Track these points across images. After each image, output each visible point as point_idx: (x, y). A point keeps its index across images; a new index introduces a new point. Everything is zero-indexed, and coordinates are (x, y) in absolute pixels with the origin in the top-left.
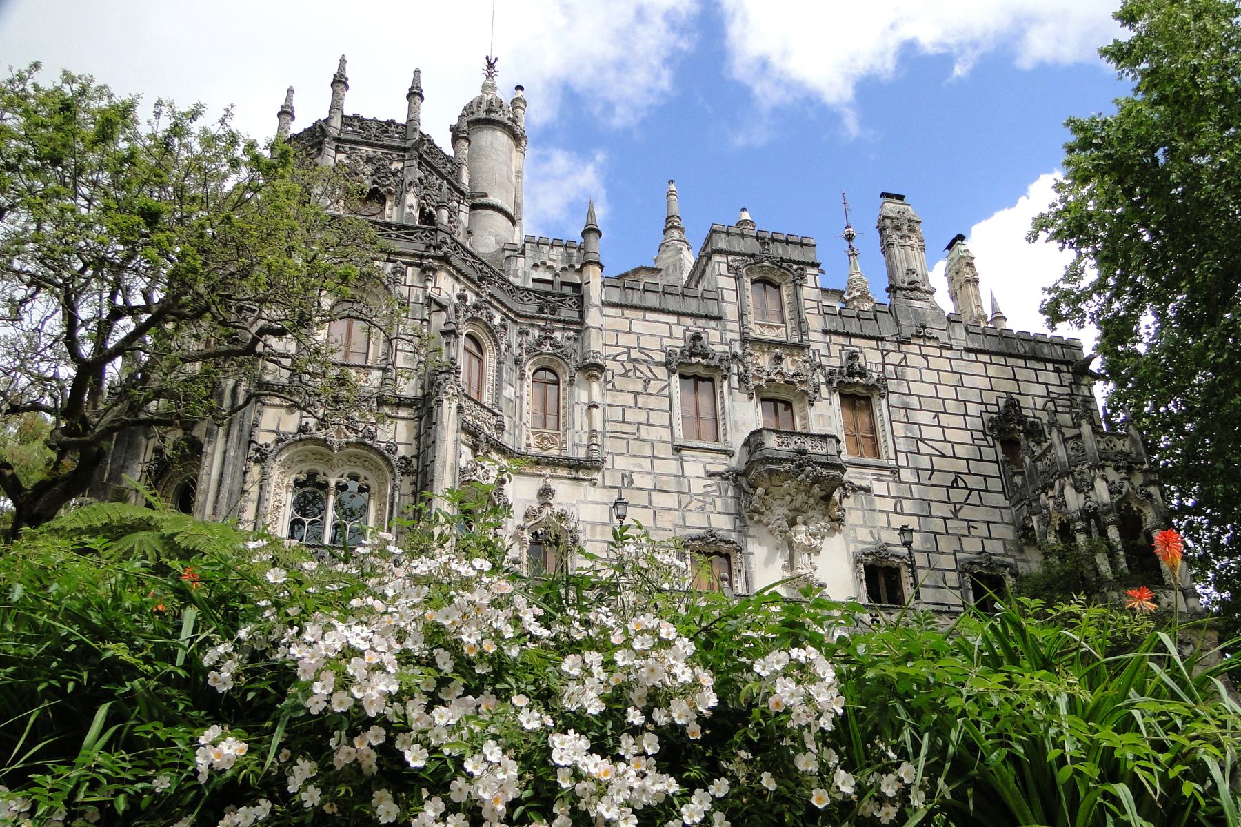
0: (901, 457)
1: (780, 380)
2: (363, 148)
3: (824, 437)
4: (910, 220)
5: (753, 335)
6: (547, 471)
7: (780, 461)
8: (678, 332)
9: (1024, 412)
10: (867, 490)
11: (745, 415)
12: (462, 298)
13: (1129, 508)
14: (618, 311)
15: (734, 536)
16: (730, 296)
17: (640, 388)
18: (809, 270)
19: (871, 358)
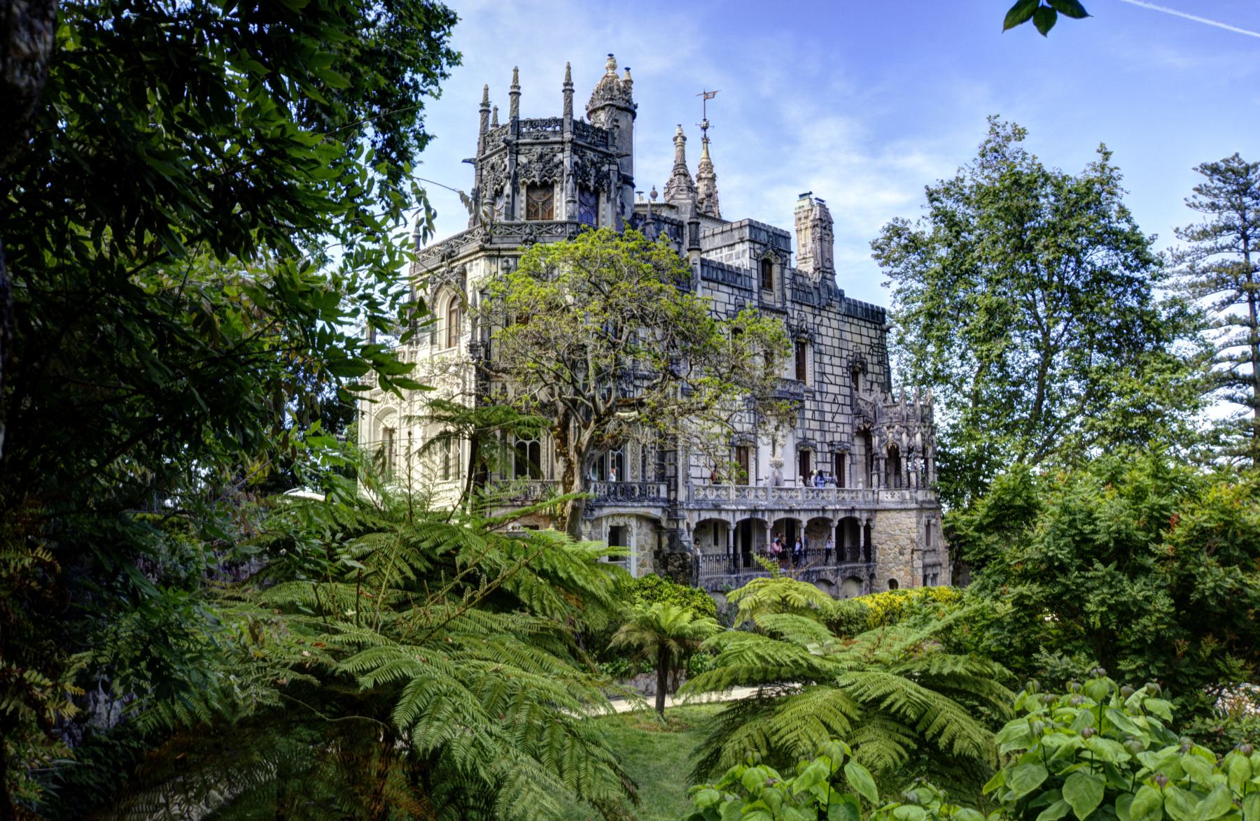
2: (588, 152)
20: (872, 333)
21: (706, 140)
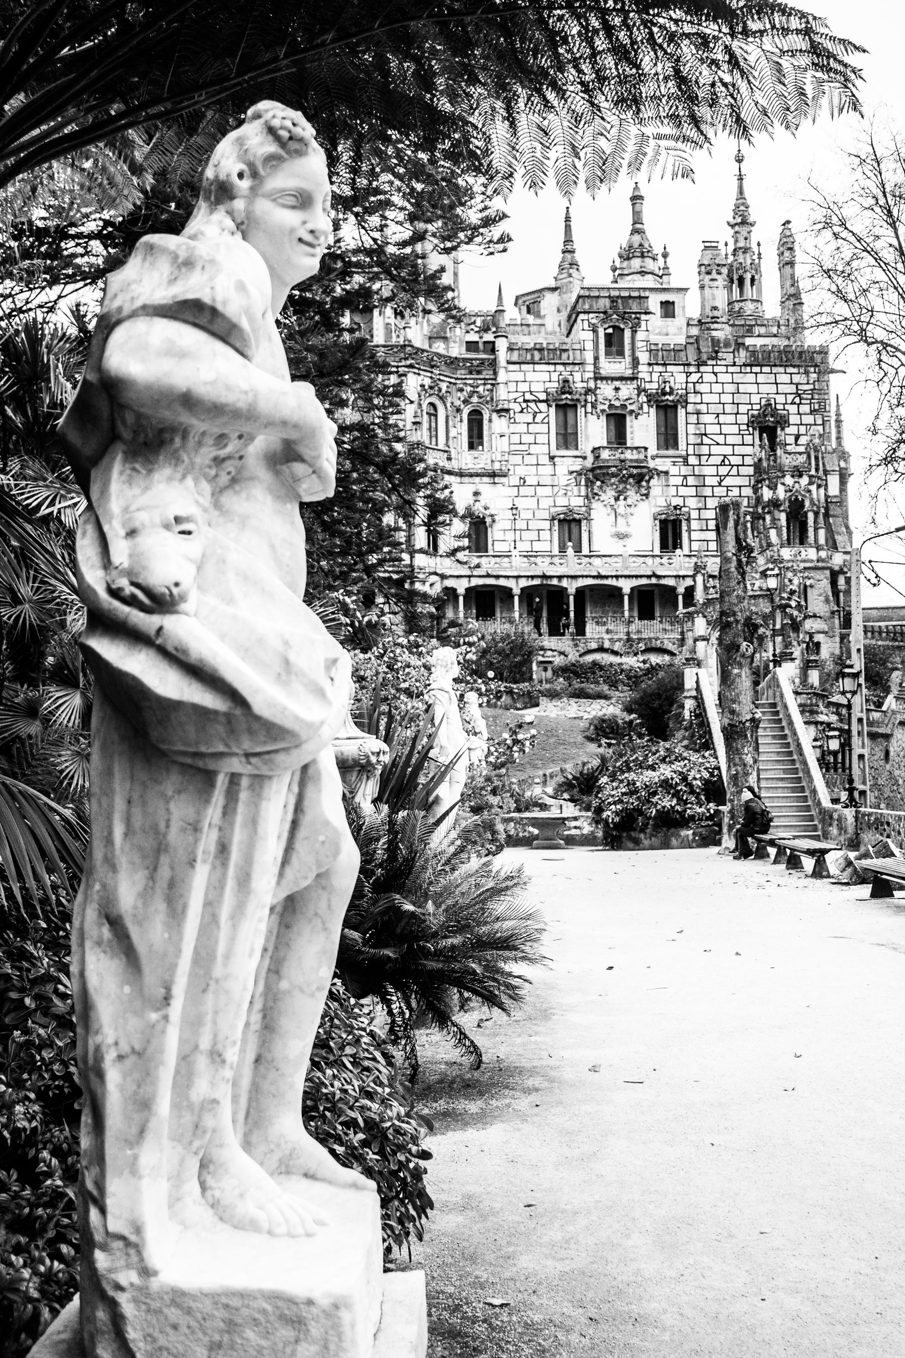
0: (691, 448)
1: (617, 404)
3: (637, 448)
4: (718, 265)
5: (603, 372)
6: (477, 480)
7: (609, 467)
8: (555, 377)
9: (778, 407)
10: (666, 473)
11: (593, 431)
12: (422, 386)
13: (797, 499)
14: (516, 367)
15: (584, 509)
16: (589, 345)
17: (531, 420)
18: (643, 317)
19: (677, 378)
20: (802, 379)
21: (741, 178)
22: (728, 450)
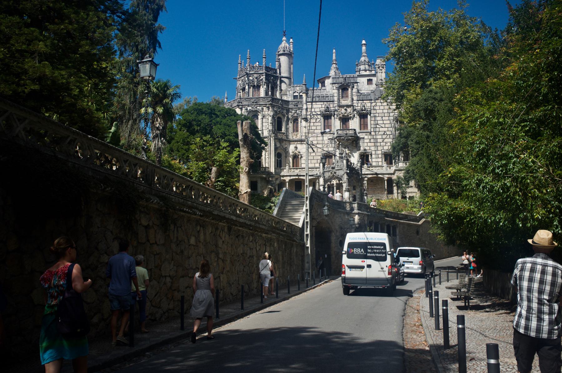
8: (323, 106)
10: (364, 138)
11: (336, 124)
16: (336, 95)
17: (314, 121)
19: (368, 104)
22: (386, 129)
